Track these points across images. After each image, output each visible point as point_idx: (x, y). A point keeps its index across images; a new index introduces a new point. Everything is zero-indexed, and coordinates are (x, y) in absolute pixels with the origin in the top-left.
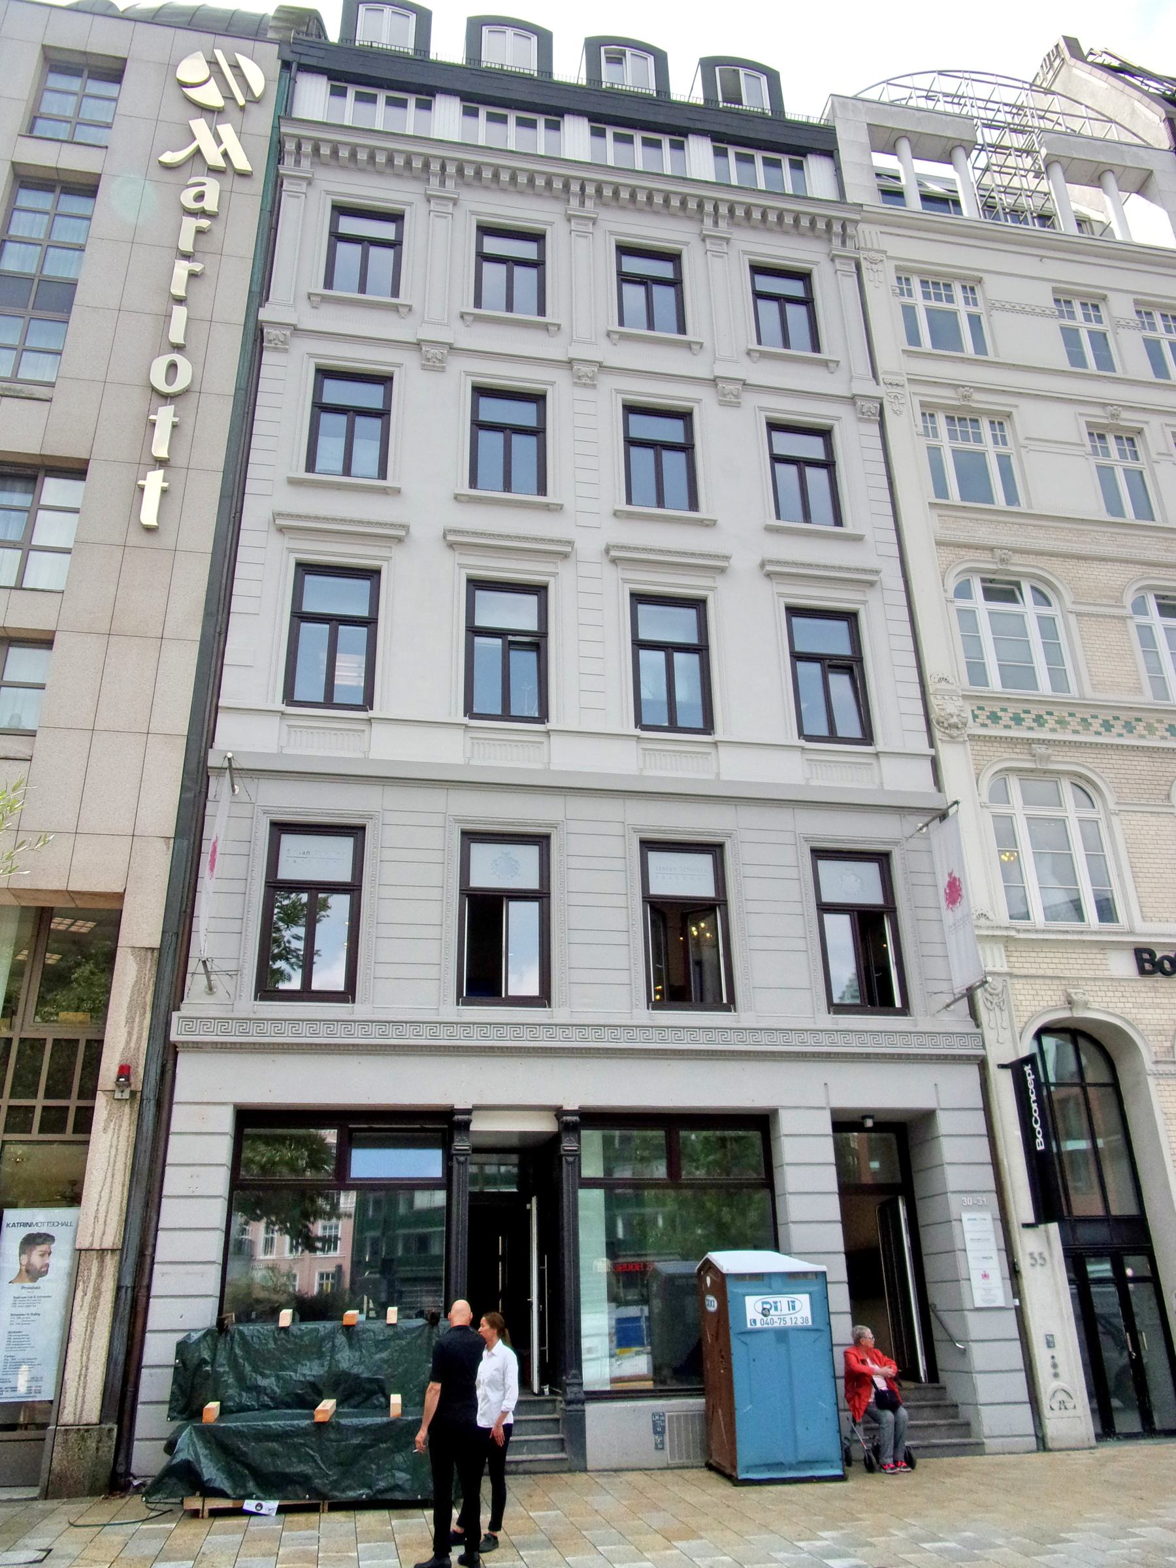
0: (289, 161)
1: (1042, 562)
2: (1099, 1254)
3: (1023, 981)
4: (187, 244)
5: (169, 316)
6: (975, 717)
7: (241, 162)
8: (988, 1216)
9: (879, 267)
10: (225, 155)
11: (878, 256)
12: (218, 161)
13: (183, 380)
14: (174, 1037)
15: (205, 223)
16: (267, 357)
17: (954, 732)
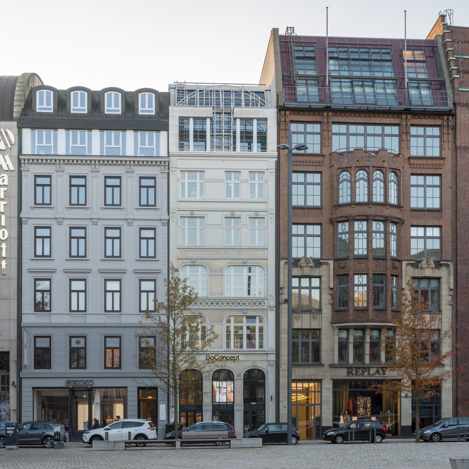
0: (23, 165)
1: (204, 261)
2: (191, 411)
4: (2, 197)
7: (12, 168)
8: (165, 405)
9: (175, 173)
10: (7, 165)
11: (175, 169)
15: (5, 189)
16: (24, 226)
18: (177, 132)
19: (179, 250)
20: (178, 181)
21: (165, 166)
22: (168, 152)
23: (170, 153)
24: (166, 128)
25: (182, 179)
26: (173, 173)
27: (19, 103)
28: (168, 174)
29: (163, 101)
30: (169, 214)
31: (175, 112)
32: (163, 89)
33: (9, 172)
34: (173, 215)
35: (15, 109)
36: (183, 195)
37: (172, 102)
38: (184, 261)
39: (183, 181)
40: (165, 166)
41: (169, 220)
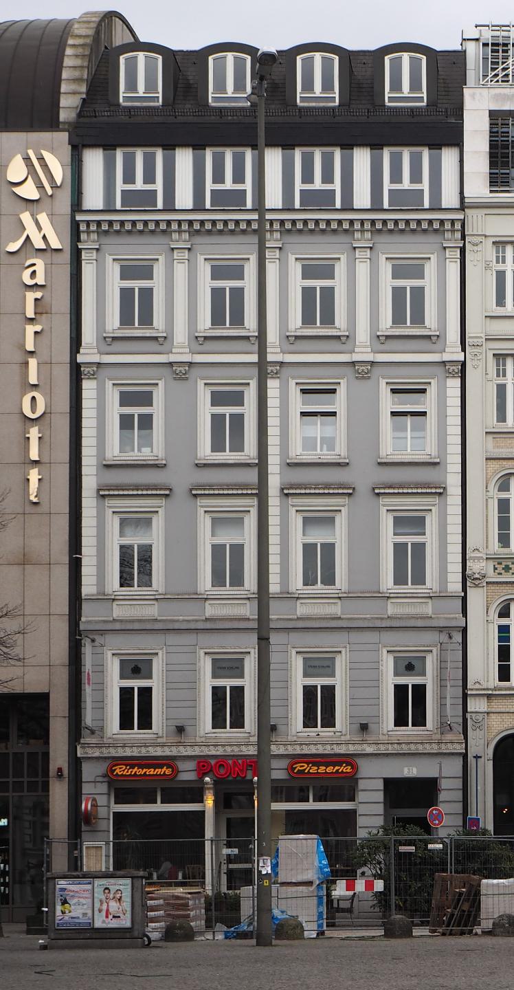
0: (83, 237)
3: (497, 715)
4: (30, 313)
5: (27, 363)
6: (495, 569)
7: (55, 243)
9: (479, 248)
10: (44, 237)
11: (480, 239)
12: (39, 244)
13: (41, 409)
14: (79, 755)
15: (39, 295)
17: (477, 582)
18: (485, 147)
19: (490, 437)
20: (487, 267)
21: (453, 231)
22: (462, 197)
23: (466, 200)
24: (455, 139)
25: (498, 262)
26: (475, 248)
27: (73, 87)
28: (463, 251)
29: (446, 70)
30: (464, 350)
31: (478, 106)
32: (444, 42)
33: (48, 254)
34: (476, 350)
35: (64, 102)
36: (501, 301)
37: (471, 75)
38: (505, 463)
39: (500, 267)
40: (453, 231)
41: (464, 364)
